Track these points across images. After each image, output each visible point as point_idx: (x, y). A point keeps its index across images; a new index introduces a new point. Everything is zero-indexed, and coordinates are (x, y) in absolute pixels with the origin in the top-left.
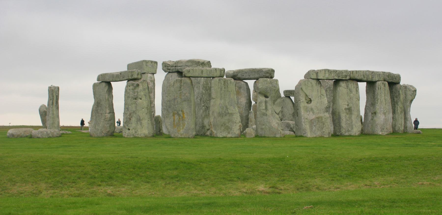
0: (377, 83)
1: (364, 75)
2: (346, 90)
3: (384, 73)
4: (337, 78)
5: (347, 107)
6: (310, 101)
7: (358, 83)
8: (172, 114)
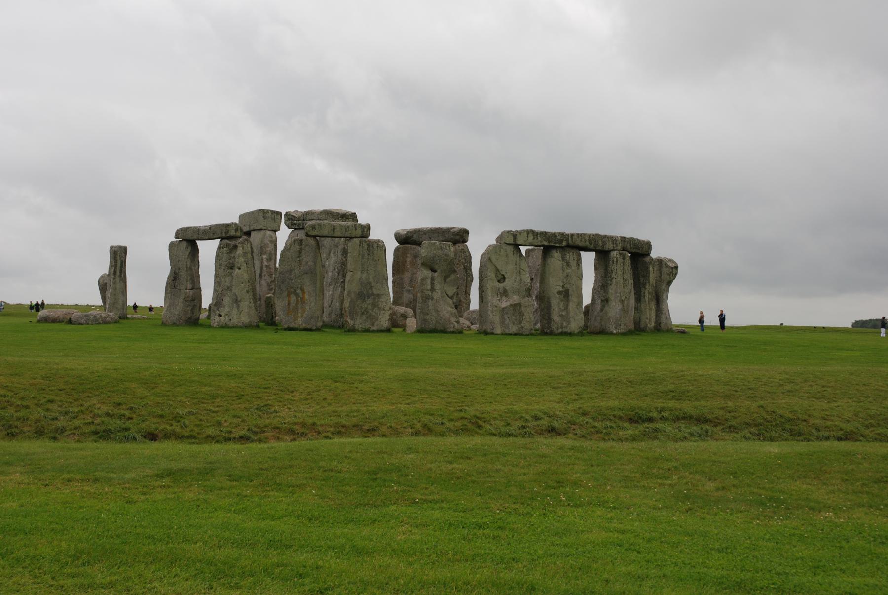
1: (589, 241)
2: (560, 263)
4: (546, 243)
5: (561, 289)
6: (502, 279)
7: (582, 253)
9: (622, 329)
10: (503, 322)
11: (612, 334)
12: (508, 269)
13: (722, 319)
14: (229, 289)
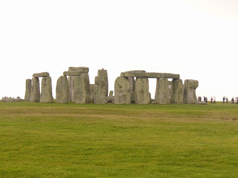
0: (160, 78)
1: (151, 75)
3: (165, 74)
5: (141, 90)
6: (121, 87)
7: (148, 78)
8: (58, 92)
10: (119, 100)
12: (123, 84)
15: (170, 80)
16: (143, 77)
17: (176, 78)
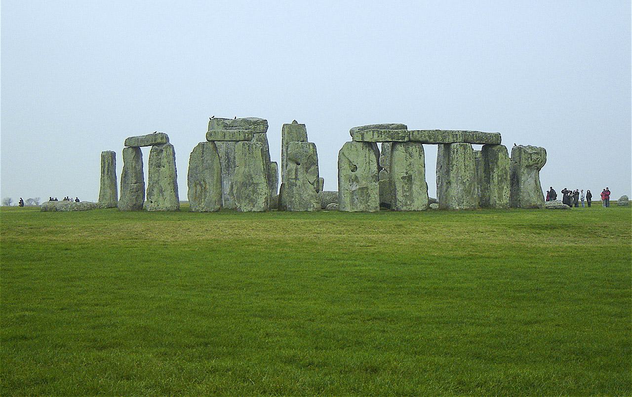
0: (452, 145)
6: (355, 169)
8: (194, 185)
9: (464, 206)
10: (352, 202)
11: (454, 210)
13: (606, 194)
14: (157, 182)
15: (478, 148)
16: (410, 141)
17: (491, 144)
